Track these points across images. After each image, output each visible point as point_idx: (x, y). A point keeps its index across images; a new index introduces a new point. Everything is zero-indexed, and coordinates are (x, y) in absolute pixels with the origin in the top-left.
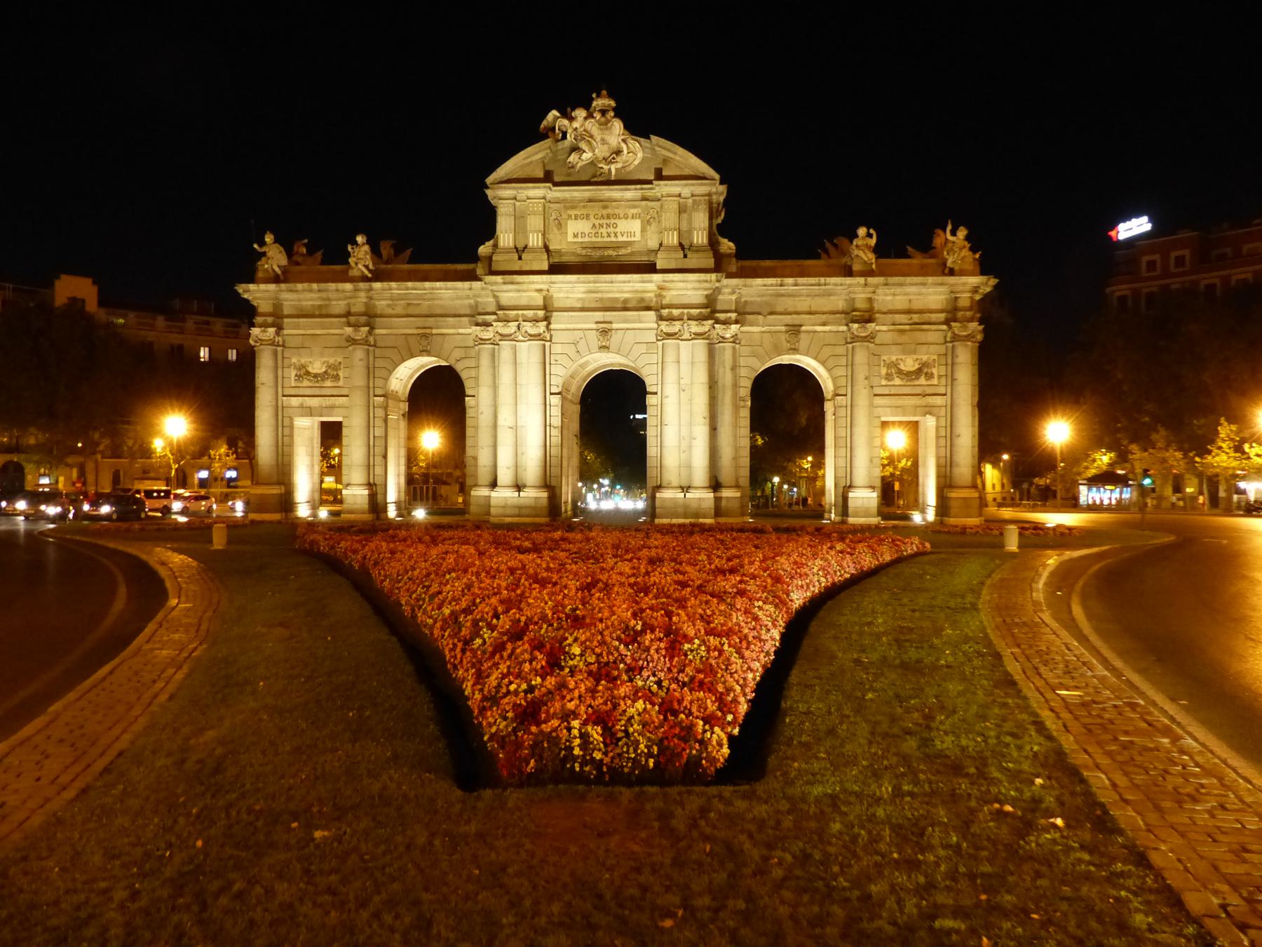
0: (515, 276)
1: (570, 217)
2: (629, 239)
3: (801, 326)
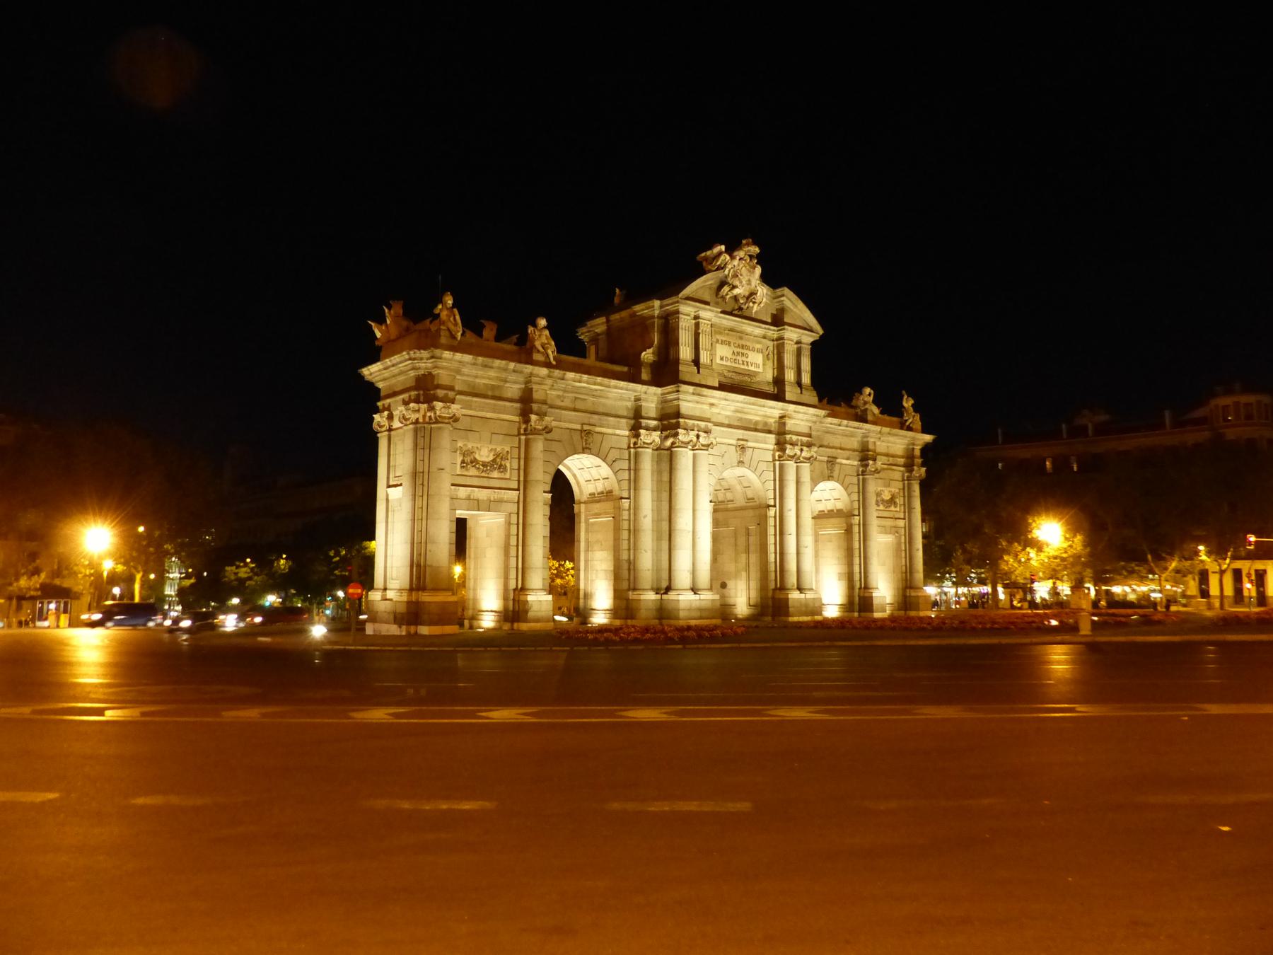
0: (704, 389)
1: (718, 341)
2: (755, 370)
3: (837, 458)
